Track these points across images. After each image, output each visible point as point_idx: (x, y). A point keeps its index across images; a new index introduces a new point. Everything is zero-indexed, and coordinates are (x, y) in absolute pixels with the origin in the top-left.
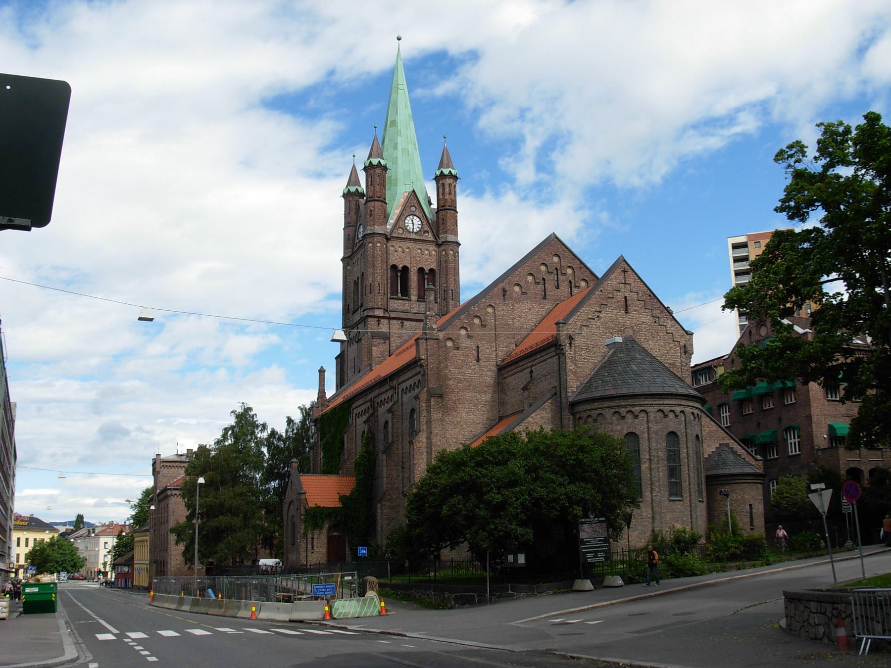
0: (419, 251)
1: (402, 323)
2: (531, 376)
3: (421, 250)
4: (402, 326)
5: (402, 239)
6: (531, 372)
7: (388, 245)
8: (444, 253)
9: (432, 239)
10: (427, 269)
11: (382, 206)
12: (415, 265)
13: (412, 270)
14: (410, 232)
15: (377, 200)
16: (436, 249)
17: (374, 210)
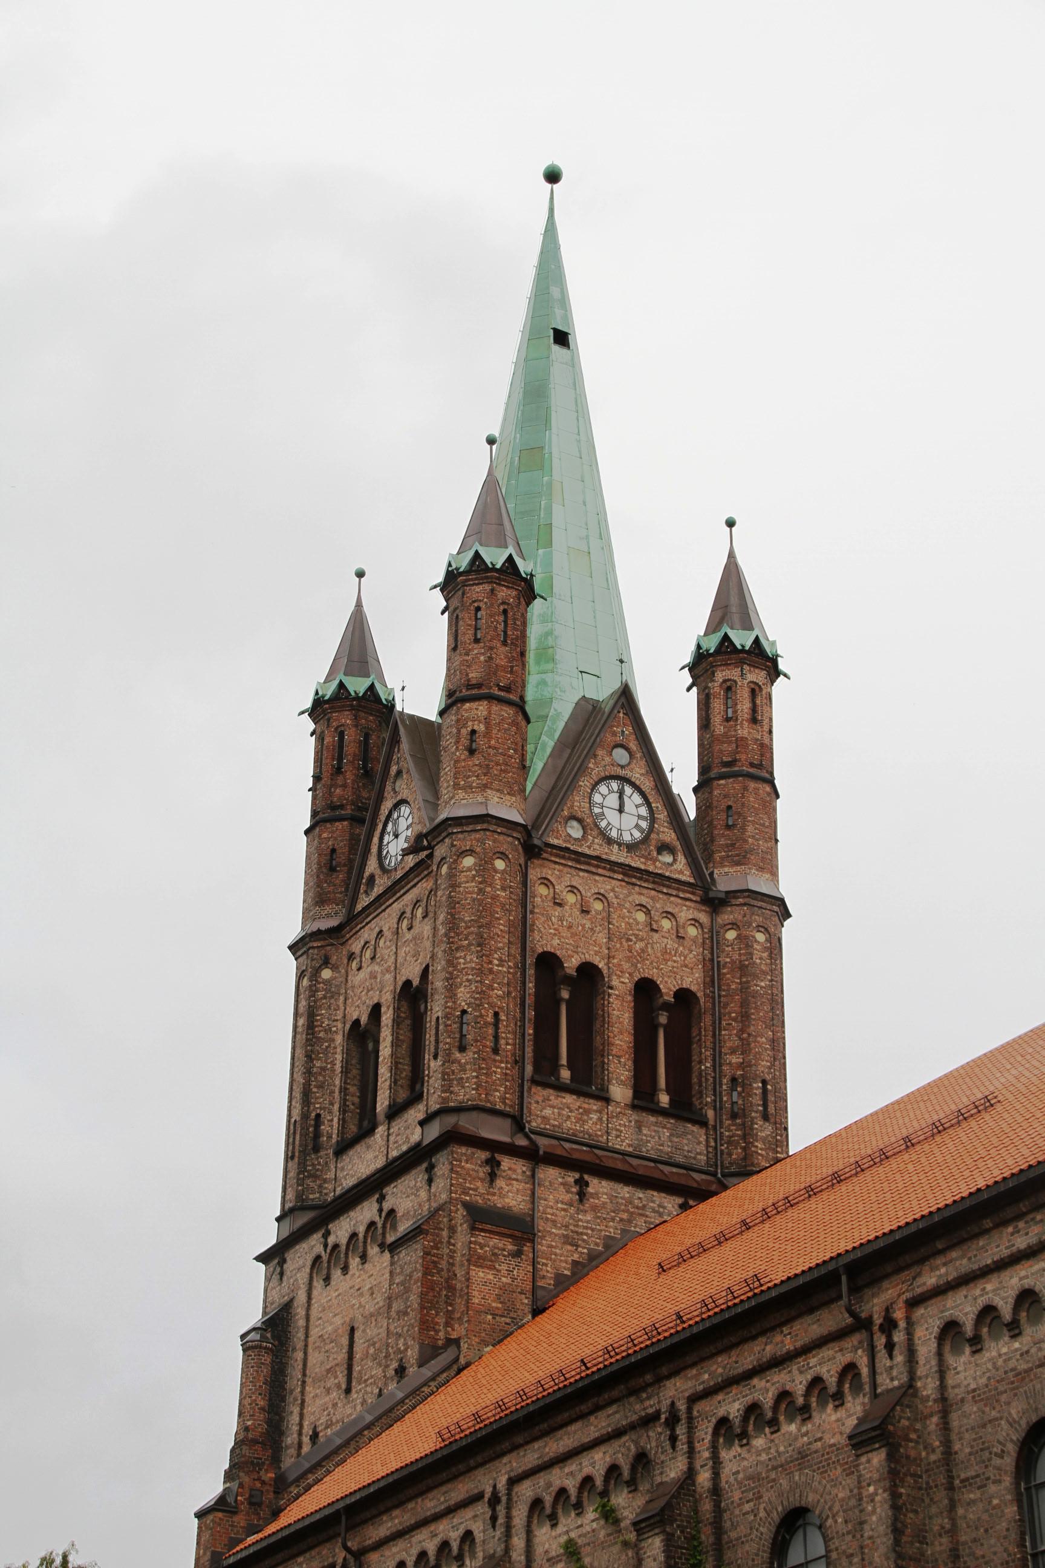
0: (641, 917)
1: (582, 1184)
3: (648, 912)
4: (582, 1195)
5: (579, 857)
7: (534, 874)
8: (731, 935)
9: (687, 876)
10: (668, 987)
11: (515, 723)
12: (626, 966)
13: (615, 982)
14: (610, 841)
15: (500, 700)
16: (704, 918)
17: (488, 734)
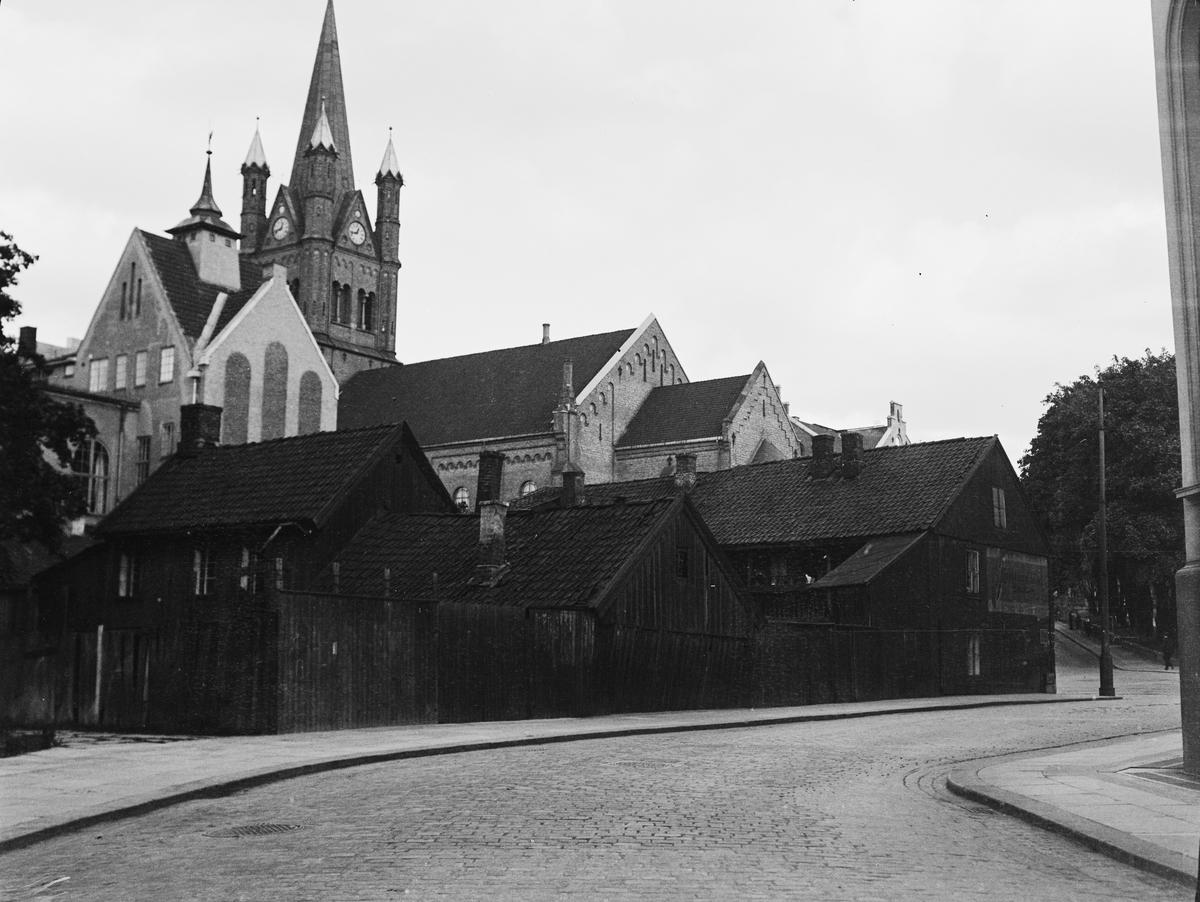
0: (361, 269)
4: (345, 359)
15: (328, 198)
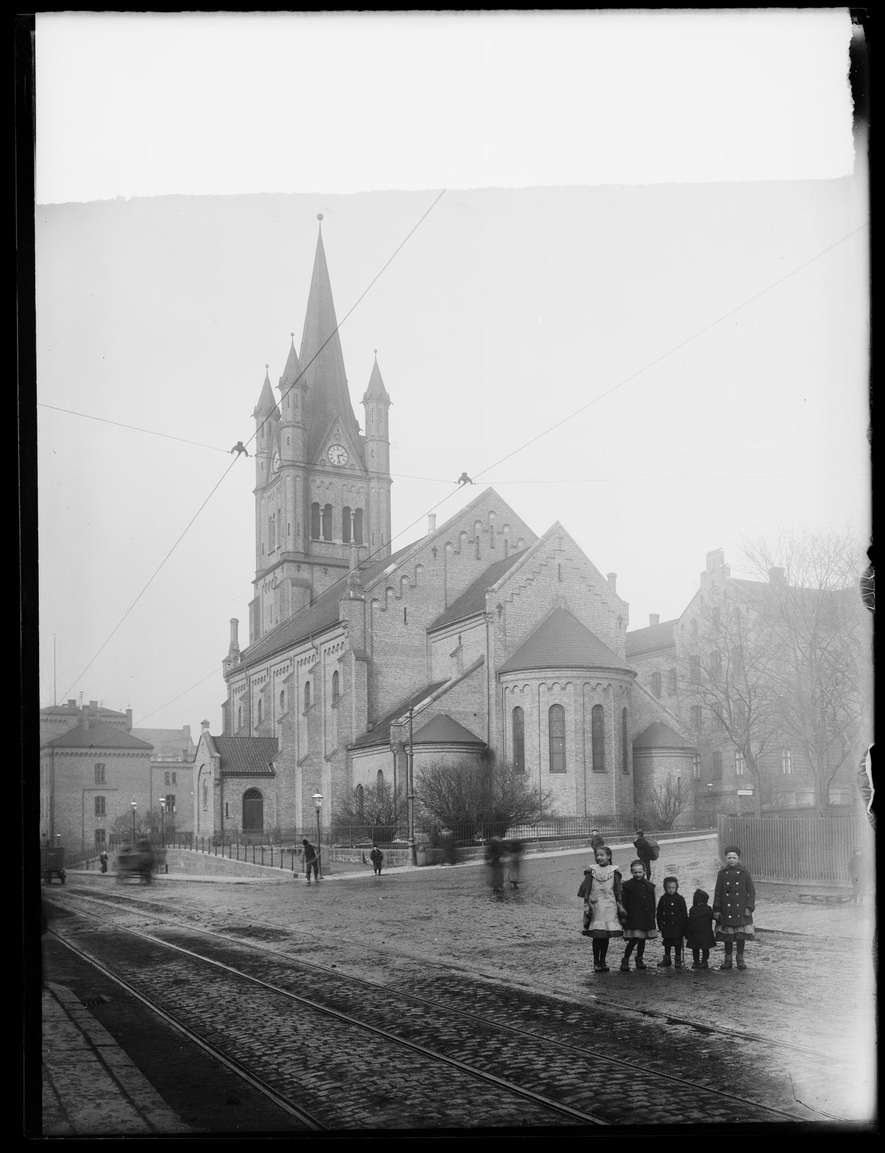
2: (460, 643)
4: (326, 573)
6: (460, 638)
